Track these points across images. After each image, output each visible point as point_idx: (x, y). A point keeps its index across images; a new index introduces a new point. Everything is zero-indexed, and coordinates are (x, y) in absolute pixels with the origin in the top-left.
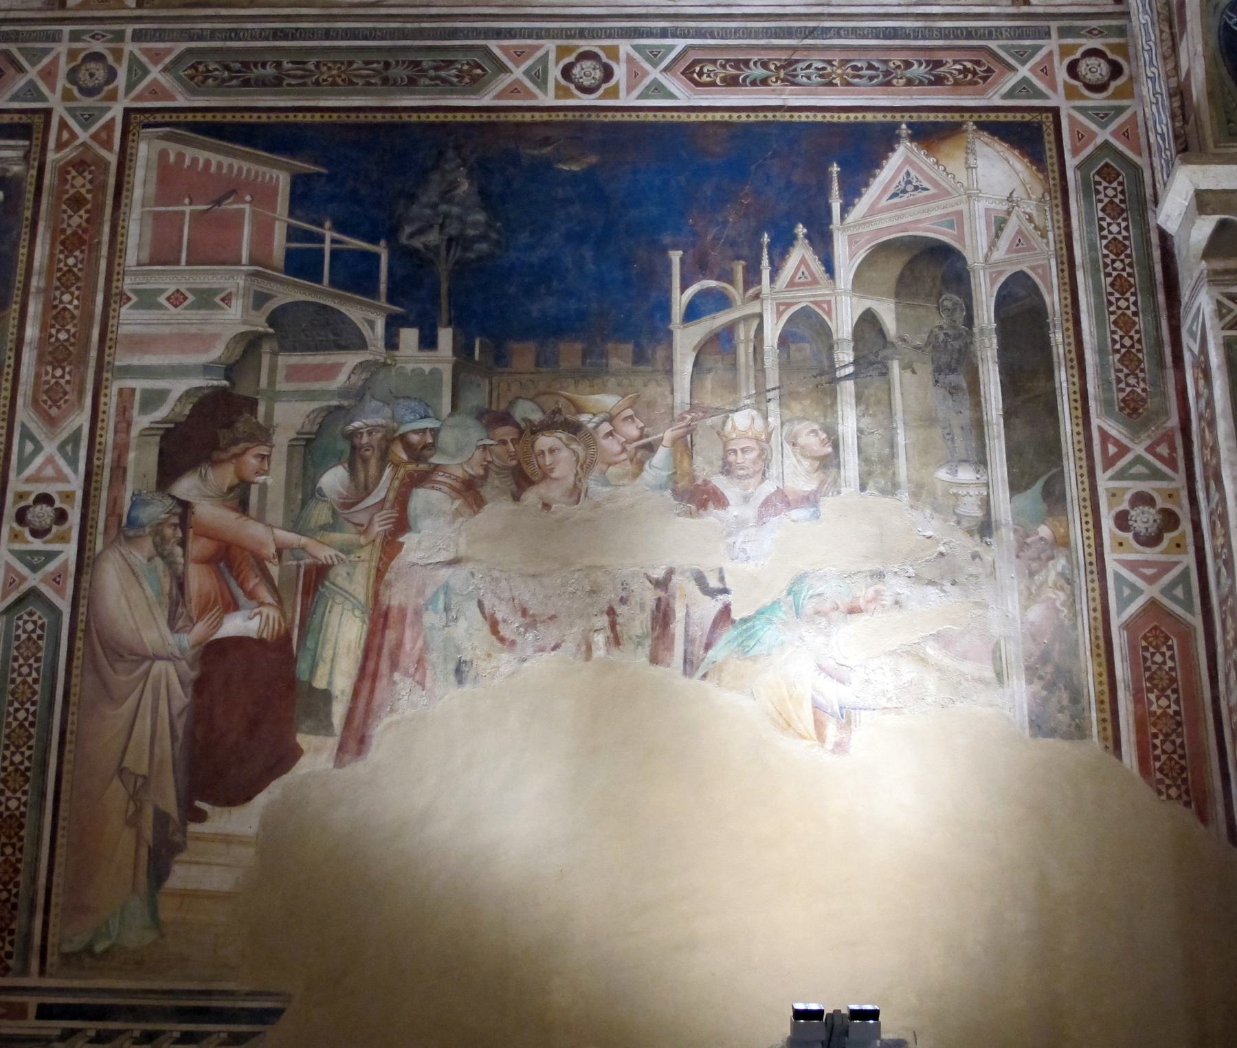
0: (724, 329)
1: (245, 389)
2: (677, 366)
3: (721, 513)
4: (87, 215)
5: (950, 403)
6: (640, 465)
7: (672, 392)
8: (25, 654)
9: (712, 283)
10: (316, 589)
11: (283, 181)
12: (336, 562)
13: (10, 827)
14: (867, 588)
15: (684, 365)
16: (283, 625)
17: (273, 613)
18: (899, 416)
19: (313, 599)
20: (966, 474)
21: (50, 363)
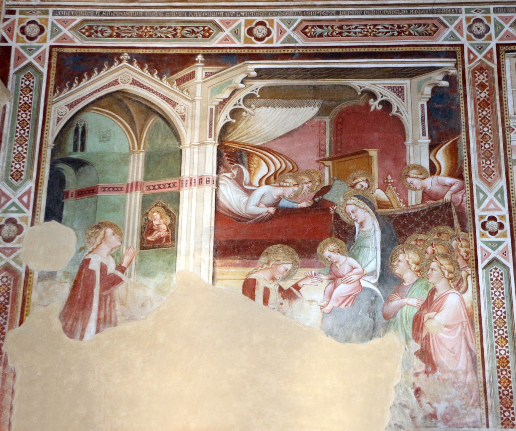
13: (503, 362)
21: (484, 158)
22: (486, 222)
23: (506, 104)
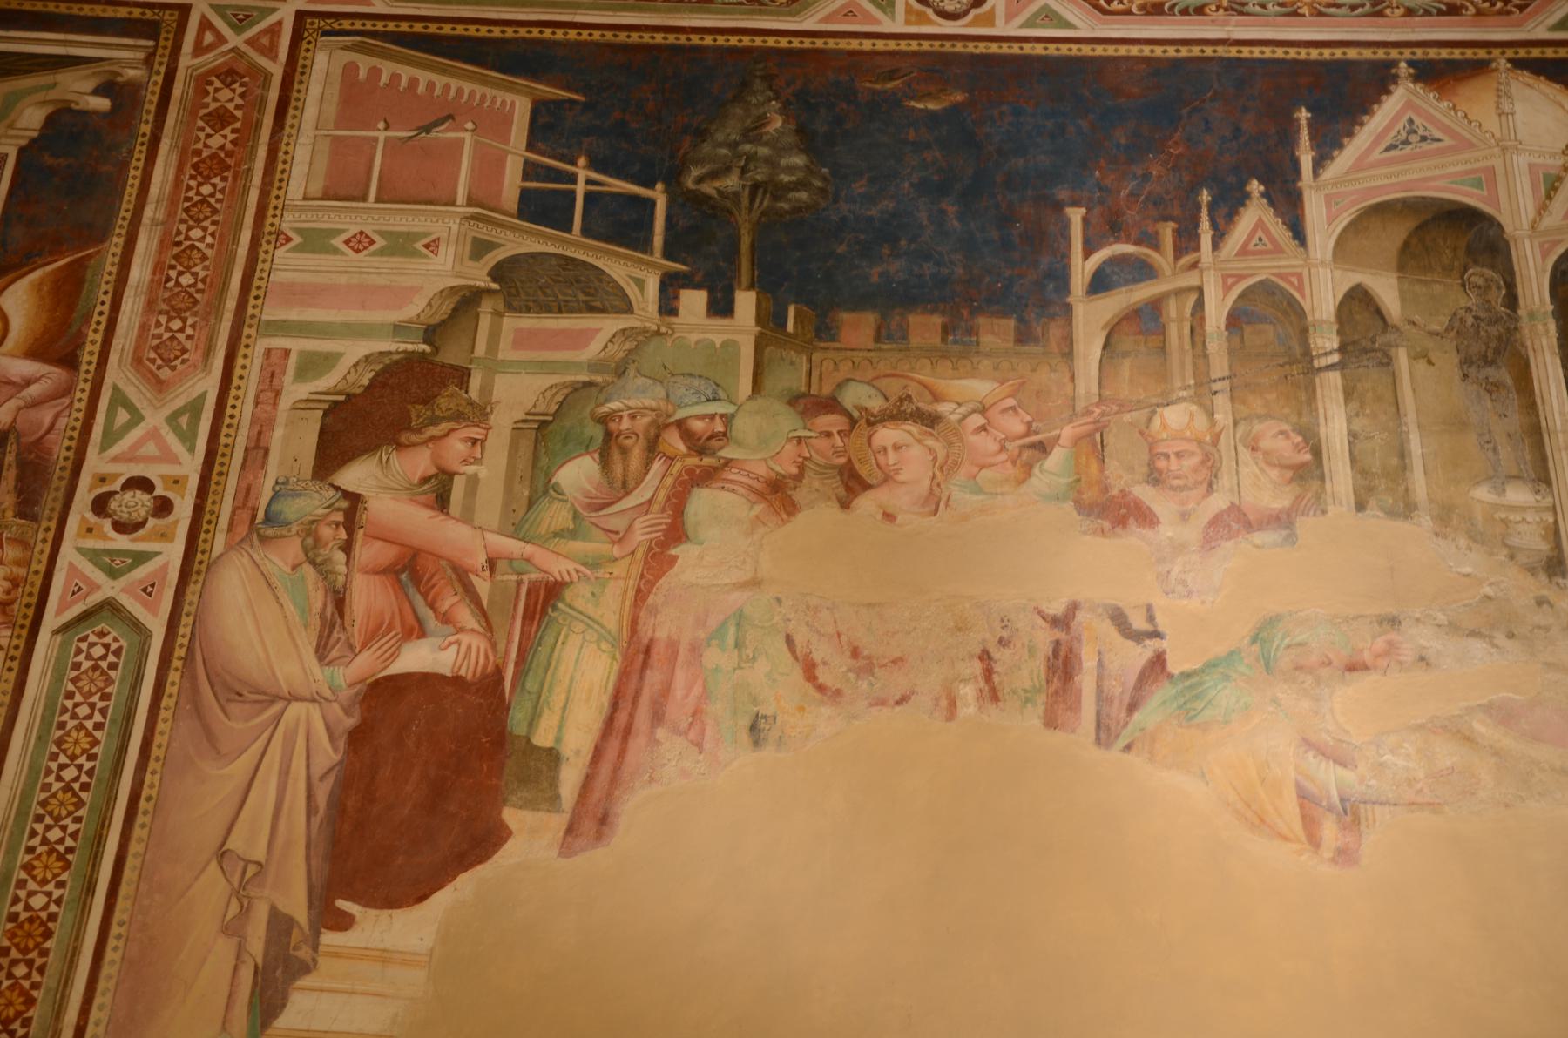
0: (1146, 304)
1: (451, 355)
2: (1079, 347)
3: (1148, 533)
4: (234, 136)
5: (1489, 404)
6: (1028, 468)
7: (1073, 378)
8: (86, 689)
9: (1128, 248)
10: (544, 612)
11: (521, 109)
12: (575, 578)
13: (29, 935)
14: (1374, 637)
15: (1089, 349)
16: (491, 658)
17: (478, 643)
18: (1411, 418)
19: (539, 626)
20: (1518, 495)
21: (167, 313)
22: (112, 494)
23: (283, 171)
